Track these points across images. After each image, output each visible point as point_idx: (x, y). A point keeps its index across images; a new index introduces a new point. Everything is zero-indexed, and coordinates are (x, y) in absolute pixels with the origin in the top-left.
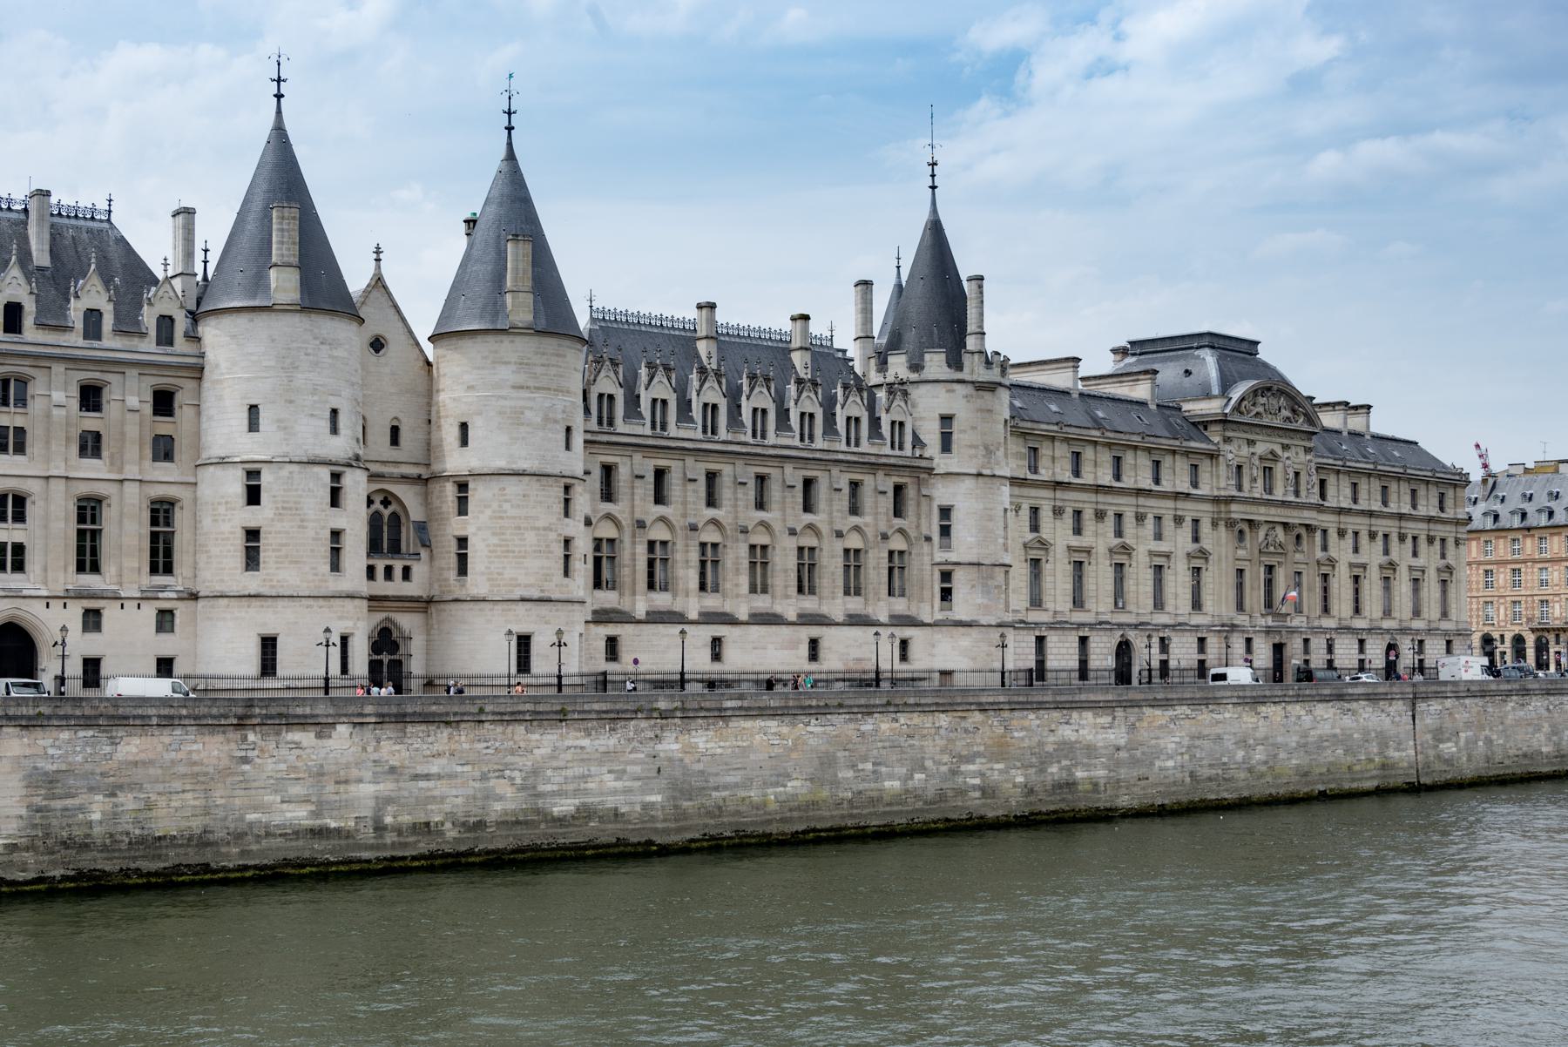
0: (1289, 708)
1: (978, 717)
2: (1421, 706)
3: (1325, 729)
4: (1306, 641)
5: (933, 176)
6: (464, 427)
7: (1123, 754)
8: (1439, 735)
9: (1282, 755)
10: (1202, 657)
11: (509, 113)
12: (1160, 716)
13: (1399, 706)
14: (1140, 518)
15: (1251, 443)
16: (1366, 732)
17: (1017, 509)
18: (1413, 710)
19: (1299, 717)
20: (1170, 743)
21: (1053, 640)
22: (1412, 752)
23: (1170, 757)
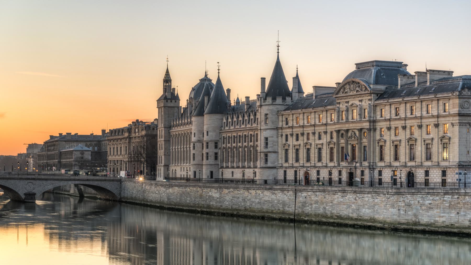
0: (257, 191)
1: (199, 189)
2: (299, 194)
3: (266, 198)
4: (362, 172)
5: (278, 49)
6: (208, 132)
7: (218, 200)
8: (304, 204)
9: (254, 204)
10: (318, 177)
11: (219, 70)
12: (226, 191)
13: (291, 193)
14: (314, 133)
15: (348, 102)
16: (279, 201)
17: (282, 135)
18: (296, 195)
19: (259, 194)
20: (228, 198)
21: (288, 171)
22: (294, 209)
23: (227, 201)
